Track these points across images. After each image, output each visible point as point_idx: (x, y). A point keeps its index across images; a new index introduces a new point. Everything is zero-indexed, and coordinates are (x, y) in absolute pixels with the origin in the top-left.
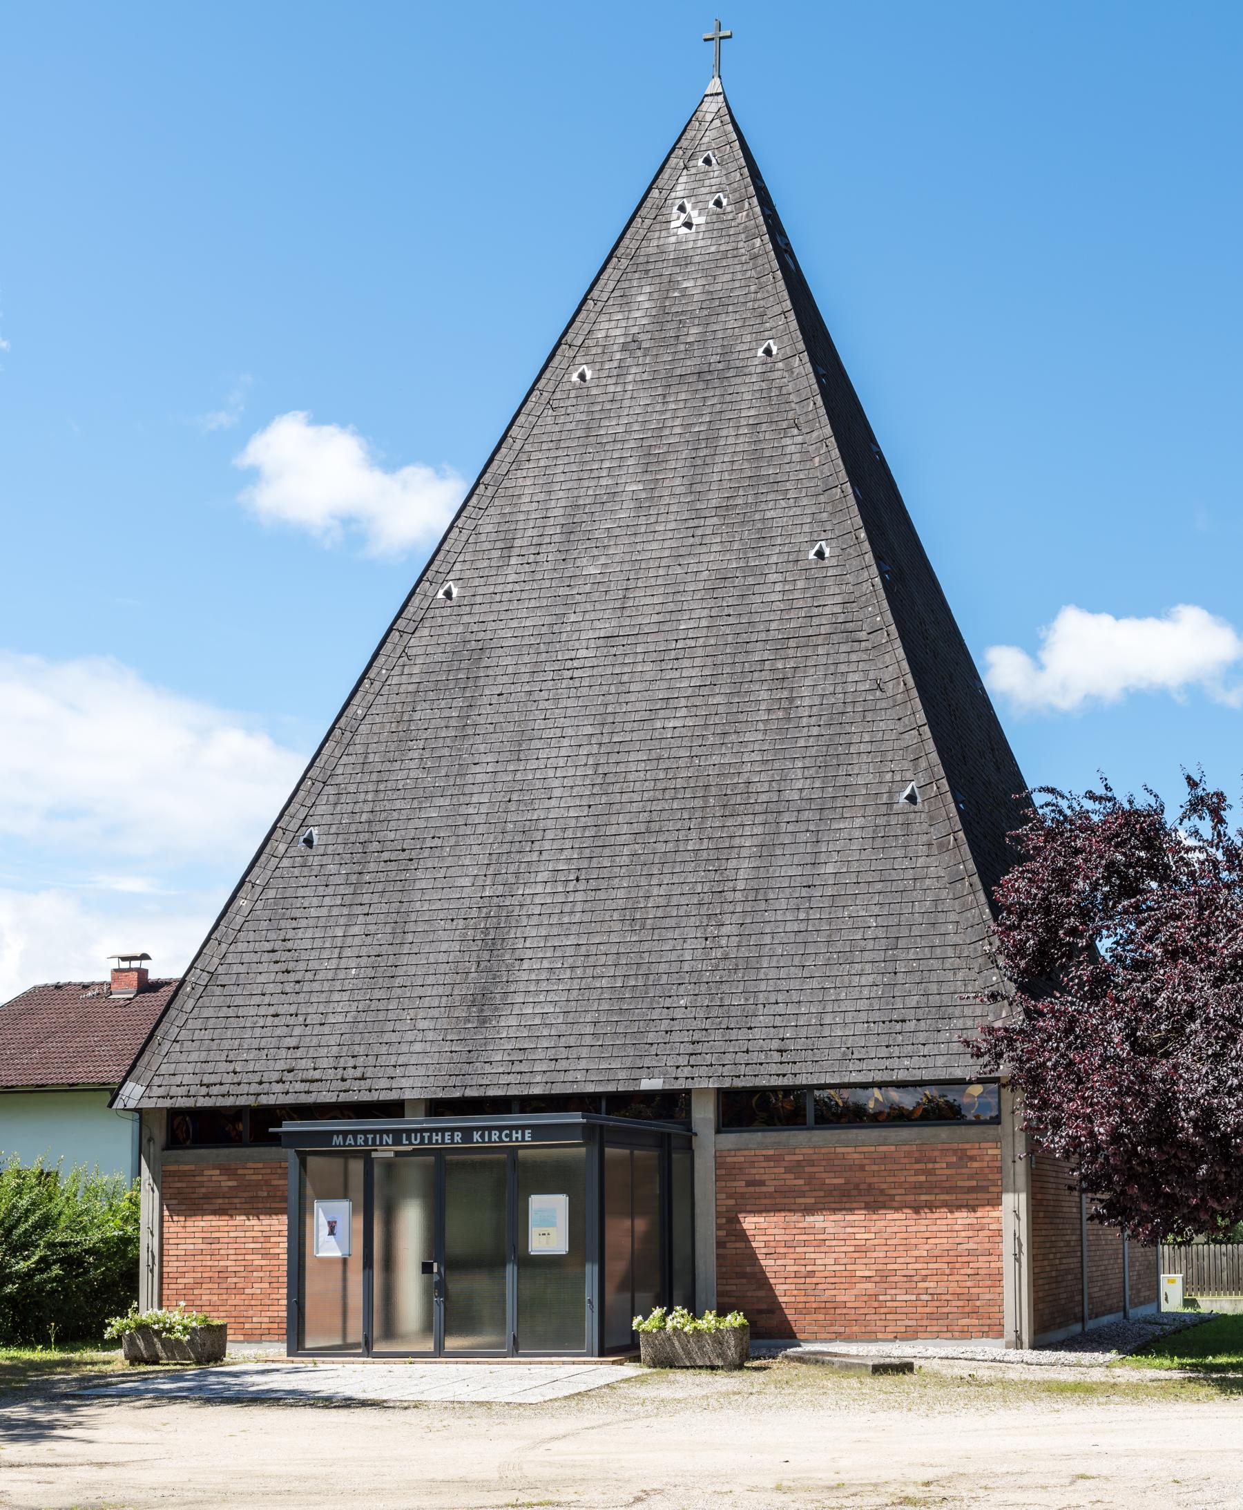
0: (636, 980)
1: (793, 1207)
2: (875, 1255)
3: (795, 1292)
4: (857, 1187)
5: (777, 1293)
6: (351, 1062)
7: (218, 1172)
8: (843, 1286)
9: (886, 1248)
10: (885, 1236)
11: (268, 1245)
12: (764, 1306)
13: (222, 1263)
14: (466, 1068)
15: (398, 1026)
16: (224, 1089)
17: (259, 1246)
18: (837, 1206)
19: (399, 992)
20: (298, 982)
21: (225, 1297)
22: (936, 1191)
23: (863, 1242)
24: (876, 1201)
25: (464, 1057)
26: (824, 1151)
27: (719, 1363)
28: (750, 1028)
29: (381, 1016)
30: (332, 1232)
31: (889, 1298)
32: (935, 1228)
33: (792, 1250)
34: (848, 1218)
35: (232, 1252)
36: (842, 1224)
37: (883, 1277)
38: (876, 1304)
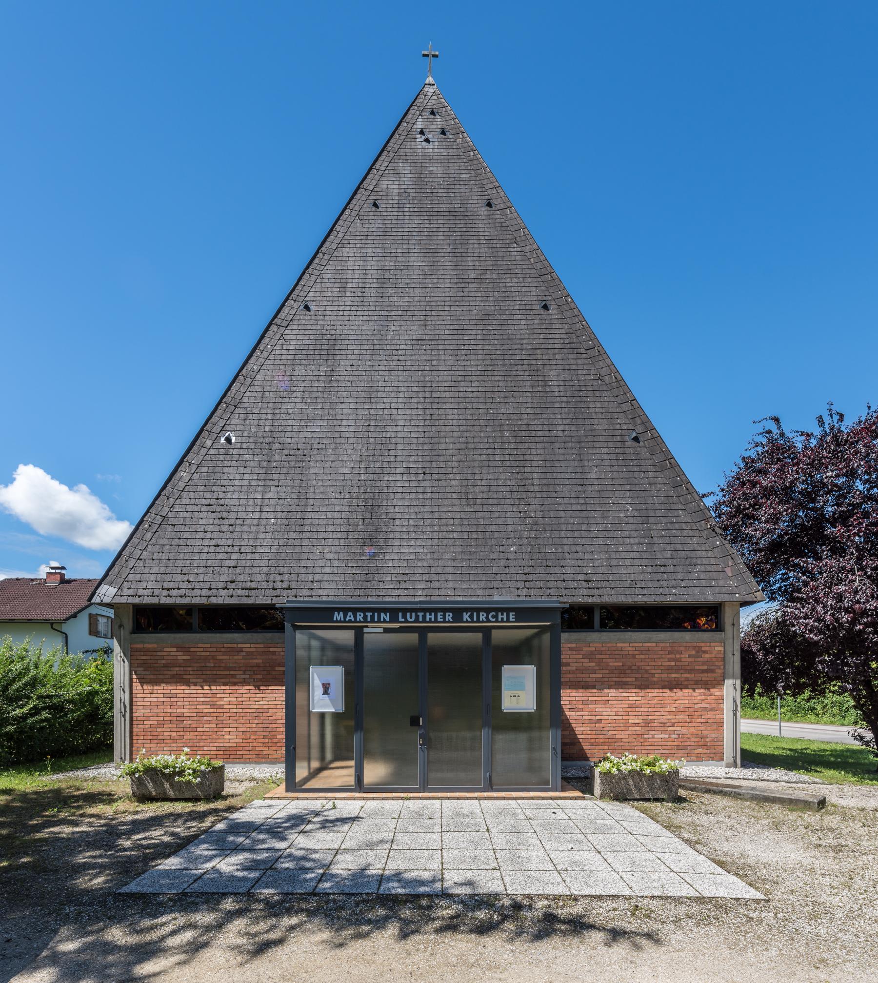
2: (641, 710)
4: (630, 668)
5: (577, 733)
6: (279, 578)
7: (175, 649)
9: (648, 706)
10: (648, 698)
11: (215, 699)
12: (567, 741)
13: (179, 711)
14: (366, 585)
15: (311, 556)
17: (208, 699)
19: (308, 535)
20: (231, 525)
21: (182, 733)
25: (363, 578)
26: (608, 645)
29: (297, 549)
35: (187, 703)
37: (647, 723)
38: (642, 740)
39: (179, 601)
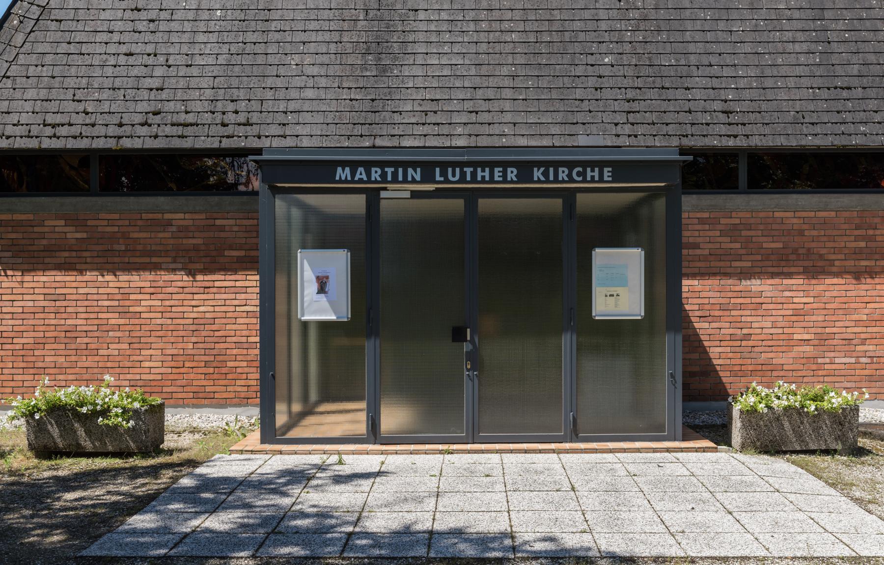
0: (551, 36)
1: (729, 270)
2: (814, 318)
3: (731, 355)
4: (795, 251)
5: (712, 355)
6: (231, 107)
7: (62, 222)
8: (780, 349)
9: (825, 312)
10: (824, 300)
11: (127, 303)
12: (696, 369)
13: (69, 322)
14: (371, 118)
15: (282, 71)
16: (76, 130)
17: (116, 303)
18: (775, 270)
19: (277, 36)
20: (152, 21)
21: (73, 358)
22: (877, 256)
23: (802, 306)
24: (815, 267)
25: (367, 106)
26: (762, 215)
27: (839, 447)
28: (687, 89)
29: (260, 60)
30: (322, 290)
31: (828, 360)
32: (874, 293)
33: (727, 313)
34: (785, 281)
35: (83, 309)
36: (780, 288)
37: (822, 340)
38: (814, 367)
39: (71, 144)
